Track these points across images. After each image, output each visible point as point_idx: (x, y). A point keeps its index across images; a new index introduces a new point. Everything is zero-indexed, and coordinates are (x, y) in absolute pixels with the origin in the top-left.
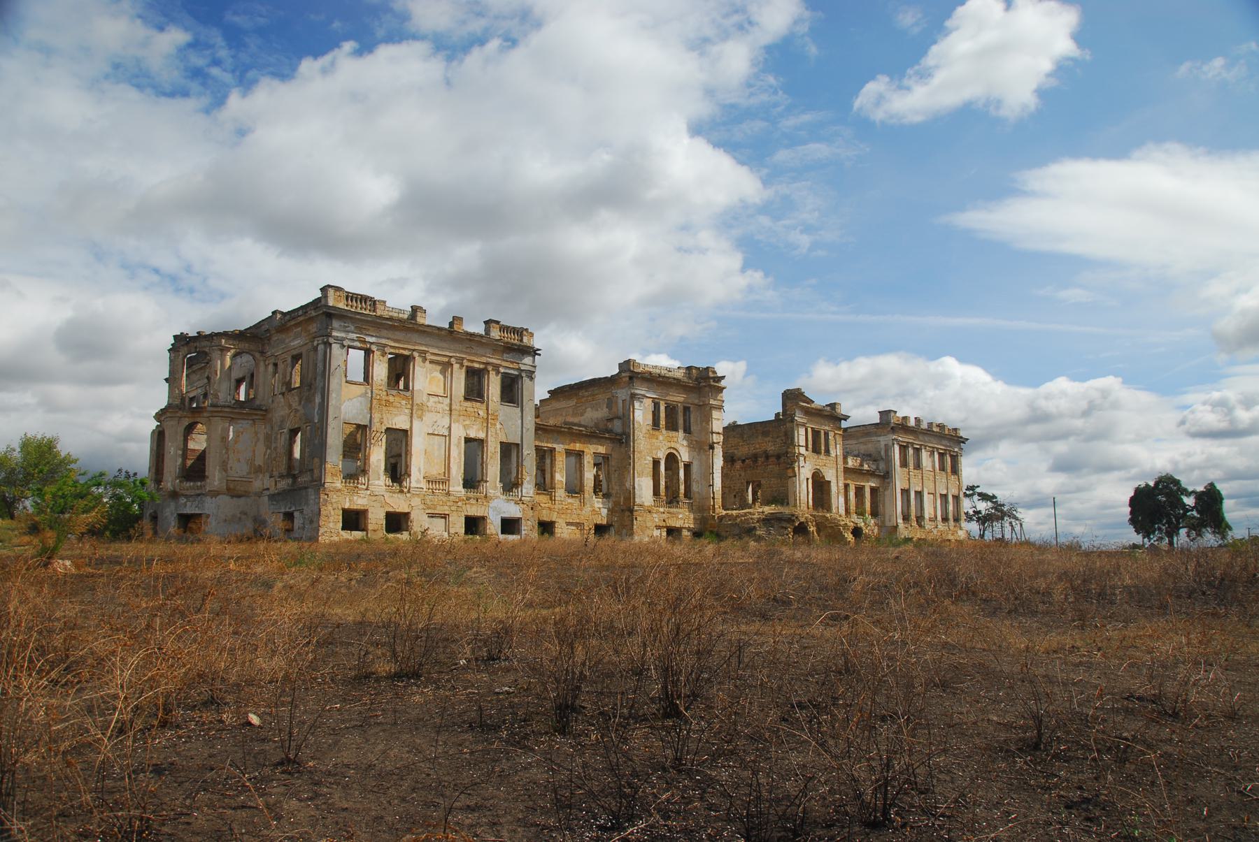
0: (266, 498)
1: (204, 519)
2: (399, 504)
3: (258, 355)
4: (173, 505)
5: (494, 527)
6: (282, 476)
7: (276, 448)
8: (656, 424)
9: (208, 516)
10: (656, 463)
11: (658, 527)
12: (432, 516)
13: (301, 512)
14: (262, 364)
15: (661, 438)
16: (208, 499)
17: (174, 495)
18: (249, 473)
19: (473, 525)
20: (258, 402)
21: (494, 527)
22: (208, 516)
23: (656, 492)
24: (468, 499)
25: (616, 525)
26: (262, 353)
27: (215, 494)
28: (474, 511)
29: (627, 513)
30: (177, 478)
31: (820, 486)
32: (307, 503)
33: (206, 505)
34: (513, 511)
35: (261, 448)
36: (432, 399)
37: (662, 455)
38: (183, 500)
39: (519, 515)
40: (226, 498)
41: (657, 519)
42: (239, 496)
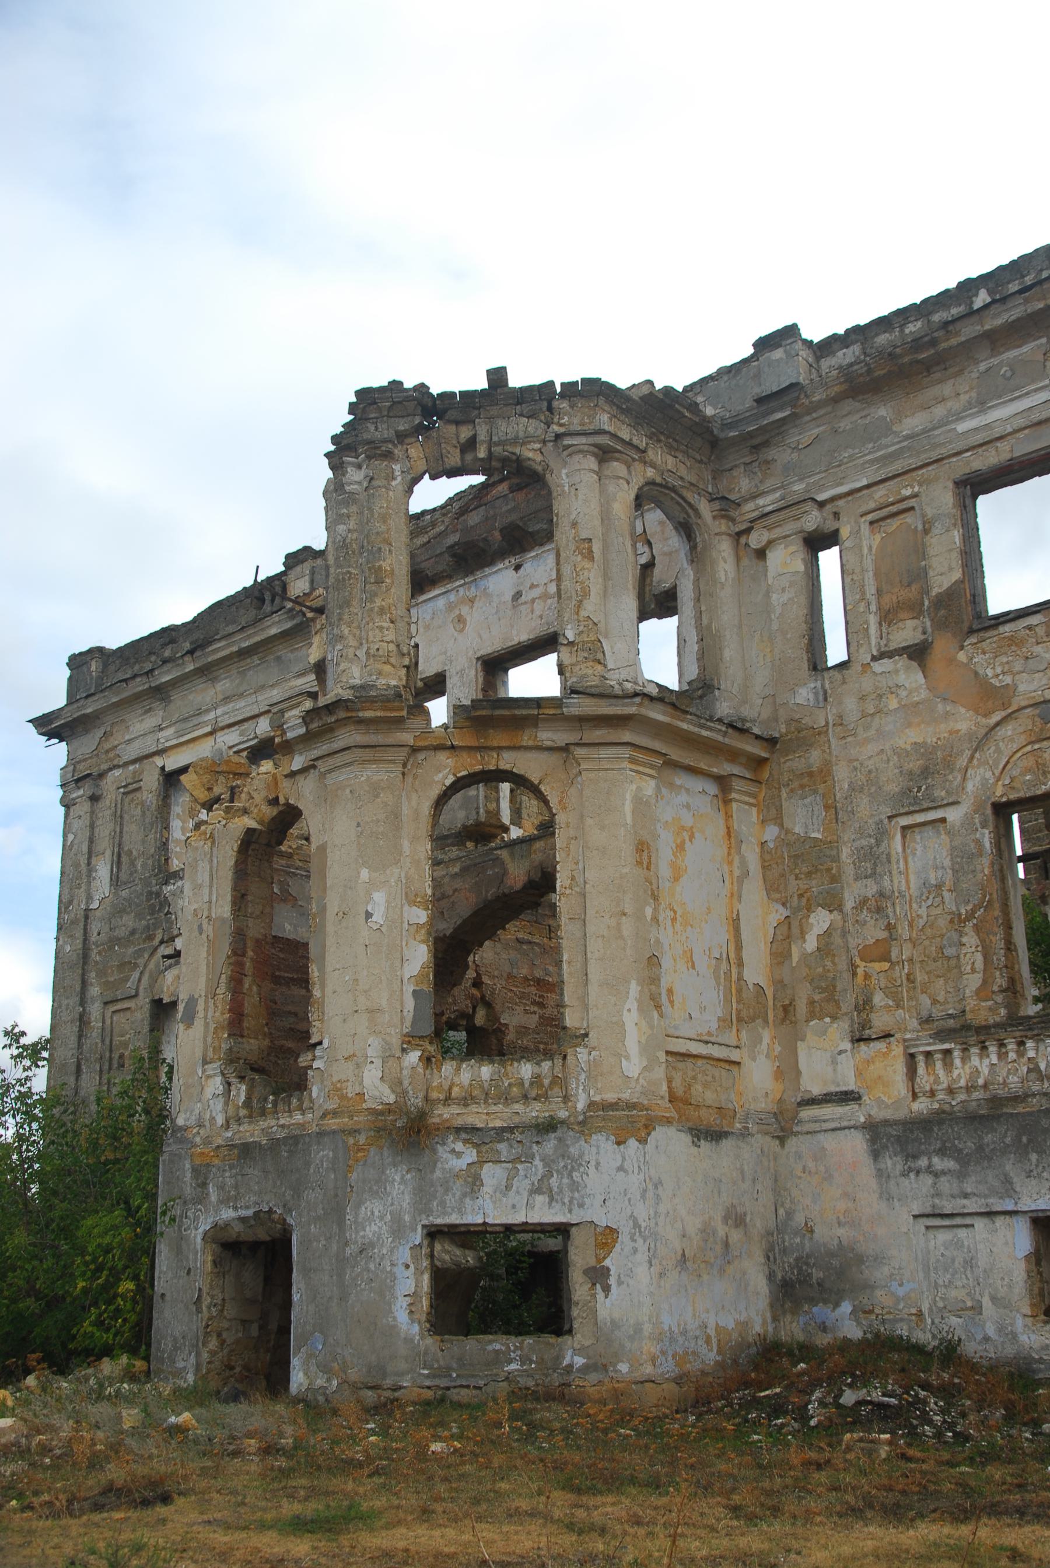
0: (856, 1144)
1: (580, 1257)
3: (705, 508)
4: (400, 1184)
6: (964, 1032)
7: (878, 905)
9: (607, 1238)
14: (724, 548)
16: (601, 1150)
17: (410, 1132)
18: (725, 1022)
20: (724, 708)
22: (607, 1238)
26: (726, 506)
27: (628, 1121)
30: (410, 1040)
33: (594, 1181)
35: (761, 917)
38: (456, 1156)
40: (670, 1143)
42: (716, 1136)
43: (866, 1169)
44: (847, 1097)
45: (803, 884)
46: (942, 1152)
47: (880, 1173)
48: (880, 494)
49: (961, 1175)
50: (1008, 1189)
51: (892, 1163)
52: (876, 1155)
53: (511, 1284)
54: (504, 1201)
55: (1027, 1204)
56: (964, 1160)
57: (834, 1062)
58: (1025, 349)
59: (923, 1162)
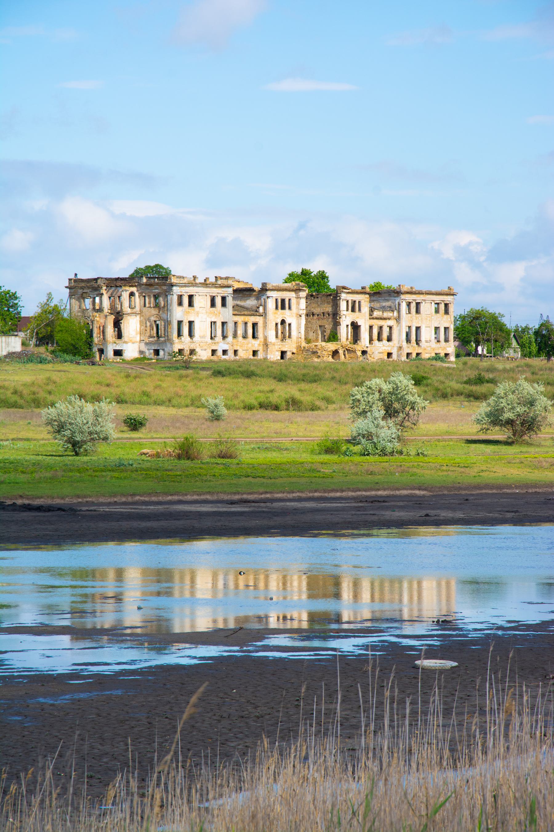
2: (192, 346)
5: (220, 353)
8: (277, 308)
10: (277, 324)
11: (277, 351)
13: (163, 350)
15: (279, 313)
19: (214, 352)
21: (220, 353)
23: (277, 337)
28: (214, 348)
31: (355, 327)
32: (166, 346)
34: (226, 347)
36: (201, 309)
37: (279, 321)
41: (277, 347)
53: (118, 353)
54: (118, 348)
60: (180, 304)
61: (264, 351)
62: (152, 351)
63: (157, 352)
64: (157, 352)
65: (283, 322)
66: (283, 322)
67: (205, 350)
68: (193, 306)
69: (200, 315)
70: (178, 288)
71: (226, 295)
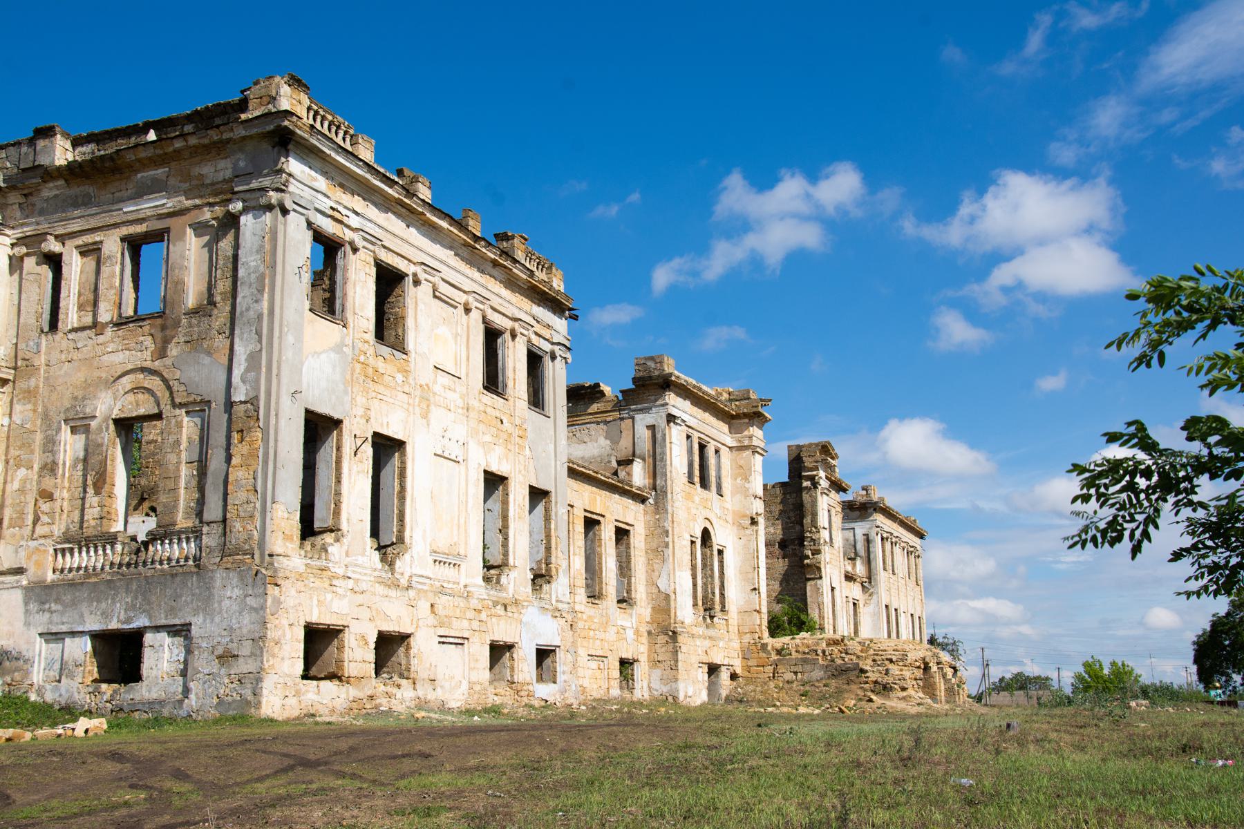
12: (444, 641)
13: (181, 631)
24: (495, 604)
25: (643, 659)
29: (662, 639)
32: (206, 603)
34: (549, 632)
36: (443, 379)
39: (556, 641)
43: (21, 609)
44: (19, 571)
45: (18, 453)
46: (57, 601)
47: (27, 611)
48: (88, 239)
49: (62, 613)
50: (83, 622)
51: (33, 607)
52: (26, 604)
55: (88, 628)
56: (65, 606)
57: (17, 552)
58: (159, 171)
59: (47, 606)
60: (328, 302)
61: (655, 663)
62: (81, 648)
63: (120, 655)
64: (120, 655)
65: (706, 535)
66: (706, 535)
67: (460, 642)
68: (399, 346)
69: (436, 414)
70: (321, 183)
71: (547, 347)
